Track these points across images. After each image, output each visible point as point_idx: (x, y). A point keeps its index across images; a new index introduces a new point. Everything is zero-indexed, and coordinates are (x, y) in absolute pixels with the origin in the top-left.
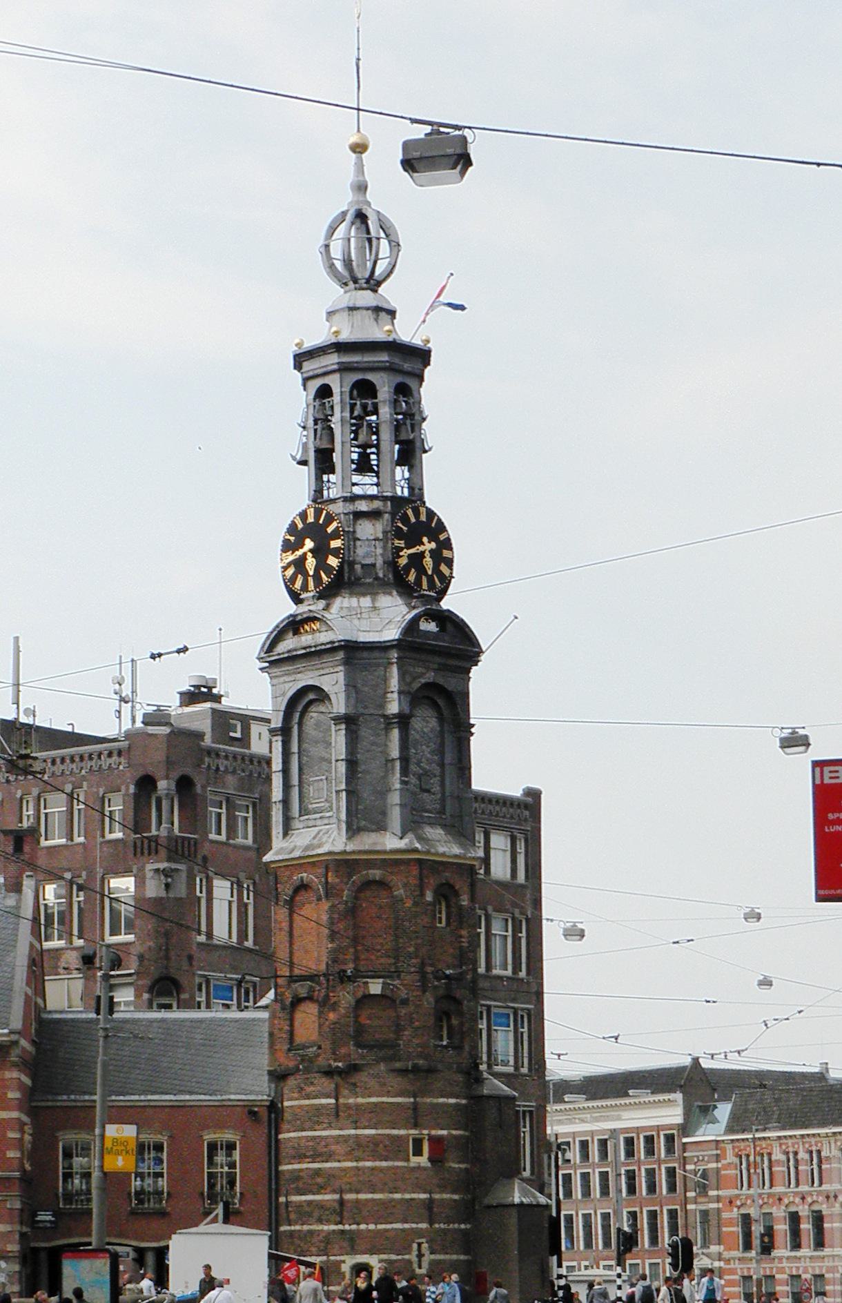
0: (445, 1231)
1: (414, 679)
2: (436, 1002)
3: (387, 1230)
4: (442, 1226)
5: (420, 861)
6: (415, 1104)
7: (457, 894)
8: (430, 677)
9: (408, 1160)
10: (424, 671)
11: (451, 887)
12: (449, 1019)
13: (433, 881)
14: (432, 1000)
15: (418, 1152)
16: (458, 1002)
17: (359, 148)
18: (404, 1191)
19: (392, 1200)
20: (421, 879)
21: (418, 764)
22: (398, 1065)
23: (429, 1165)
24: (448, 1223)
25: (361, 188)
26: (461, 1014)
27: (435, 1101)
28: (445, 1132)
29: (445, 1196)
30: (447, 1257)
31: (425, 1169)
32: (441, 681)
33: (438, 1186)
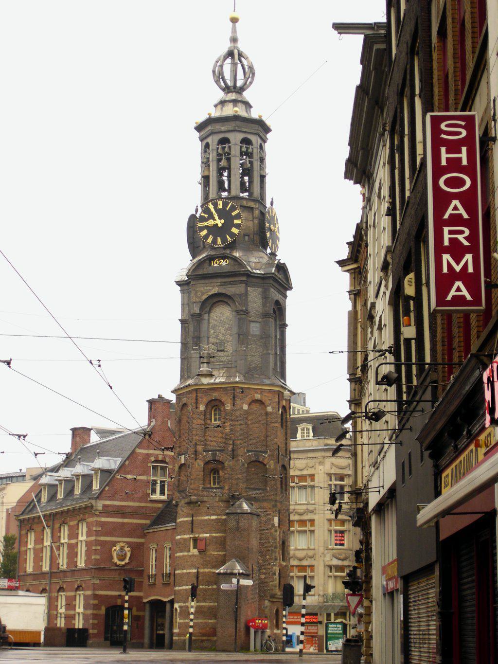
0: (205, 590)
1: (203, 294)
2: (205, 464)
3: (181, 590)
4: (204, 587)
5: (196, 390)
6: (193, 520)
7: (223, 404)
8: (215, 290)
9: (189, 551)
10: (211, 288)
11: (220, 401)
12: (218, 472)
13: (206, 400)
14: (202, 464)
15: (194, 548)
16: (222, 463)
17: (234, 20)
18: (187, 568)
19: (183, 573)
20: (197, 399)
21: (216, 337)
22: (187, 500)
23: (198, 553)
24: (209, 585)
25: (234, 40)
26: (223, 468)
27: (203, 518)
28: (208, 535)
29: (206, 570)
30: (207, 604)
31: (195, 556)
32: (222, 291)
33: (202, 565)
